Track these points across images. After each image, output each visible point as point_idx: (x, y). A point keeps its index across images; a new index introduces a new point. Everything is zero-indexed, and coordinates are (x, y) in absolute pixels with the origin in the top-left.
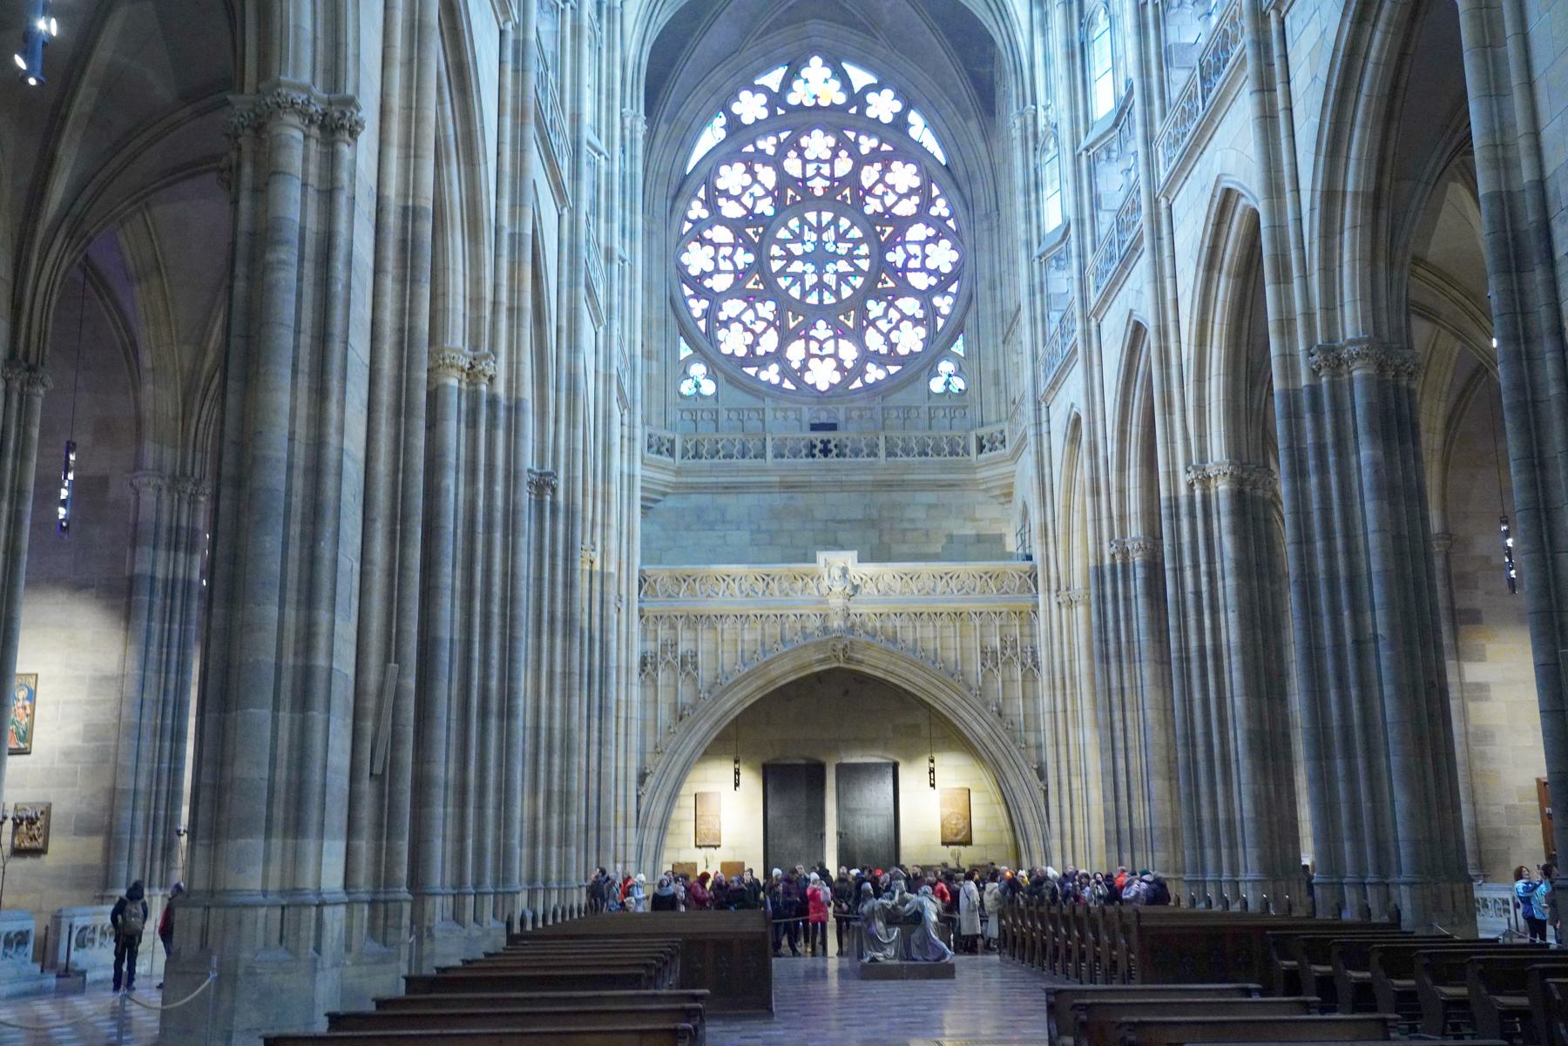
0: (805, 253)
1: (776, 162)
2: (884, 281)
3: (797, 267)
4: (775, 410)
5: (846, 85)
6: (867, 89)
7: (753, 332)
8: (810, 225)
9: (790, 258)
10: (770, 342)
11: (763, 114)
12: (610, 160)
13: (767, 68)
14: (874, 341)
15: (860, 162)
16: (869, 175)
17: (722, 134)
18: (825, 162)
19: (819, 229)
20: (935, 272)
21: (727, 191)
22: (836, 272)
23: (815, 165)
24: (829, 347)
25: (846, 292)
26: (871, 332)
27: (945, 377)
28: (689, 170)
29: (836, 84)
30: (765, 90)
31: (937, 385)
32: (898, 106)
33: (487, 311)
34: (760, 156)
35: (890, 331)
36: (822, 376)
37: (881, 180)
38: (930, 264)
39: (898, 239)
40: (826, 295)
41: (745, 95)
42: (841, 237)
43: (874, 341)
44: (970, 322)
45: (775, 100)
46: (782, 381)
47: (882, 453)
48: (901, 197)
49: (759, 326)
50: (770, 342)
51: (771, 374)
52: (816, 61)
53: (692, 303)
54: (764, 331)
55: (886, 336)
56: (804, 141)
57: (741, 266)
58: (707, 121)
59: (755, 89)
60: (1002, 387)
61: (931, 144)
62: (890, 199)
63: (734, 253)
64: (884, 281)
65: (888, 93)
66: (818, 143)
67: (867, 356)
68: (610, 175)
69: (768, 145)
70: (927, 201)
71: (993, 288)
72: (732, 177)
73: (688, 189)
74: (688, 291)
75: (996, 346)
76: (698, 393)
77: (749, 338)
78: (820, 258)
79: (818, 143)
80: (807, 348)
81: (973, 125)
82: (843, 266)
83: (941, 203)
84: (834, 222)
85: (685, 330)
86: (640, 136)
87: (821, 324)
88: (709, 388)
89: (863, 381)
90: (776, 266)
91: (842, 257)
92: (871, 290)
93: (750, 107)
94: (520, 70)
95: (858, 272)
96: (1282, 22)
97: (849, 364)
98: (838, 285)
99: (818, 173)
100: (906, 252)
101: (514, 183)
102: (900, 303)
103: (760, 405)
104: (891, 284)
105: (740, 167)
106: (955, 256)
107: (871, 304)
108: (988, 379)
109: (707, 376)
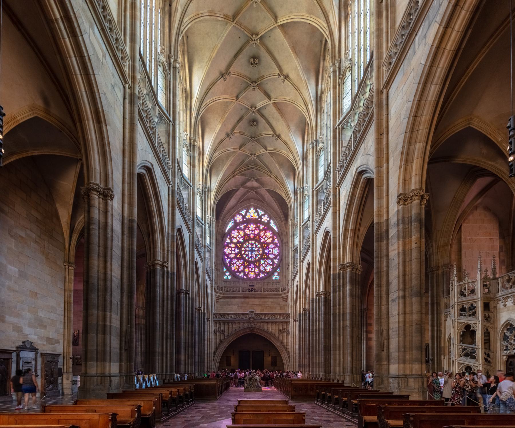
1: (243, 230)
5: (258, 214)
6: (263, 215)
11: (241, 220)
12: (205, 226)
15: (260, 231)
17: (233, 224)
29: (256, 214)
32: (268, 219)
33: (166, 252)
34: (240, 229)
41: (238, 216)
45: (244, 217)
56: (249, 226)
58: (230, 221)
65: (266, 216)
66: (252, 226)
68: (205, 229)
69: (242, 227)
72: (235, 233)
73: (226, 236)
79: (252, 226)
81: (283, 223)
86: (214, 223)
93: (239, 218)
94: (173, 197)
96: (339, 190)
101: (172, 223)
105: (236, 231)
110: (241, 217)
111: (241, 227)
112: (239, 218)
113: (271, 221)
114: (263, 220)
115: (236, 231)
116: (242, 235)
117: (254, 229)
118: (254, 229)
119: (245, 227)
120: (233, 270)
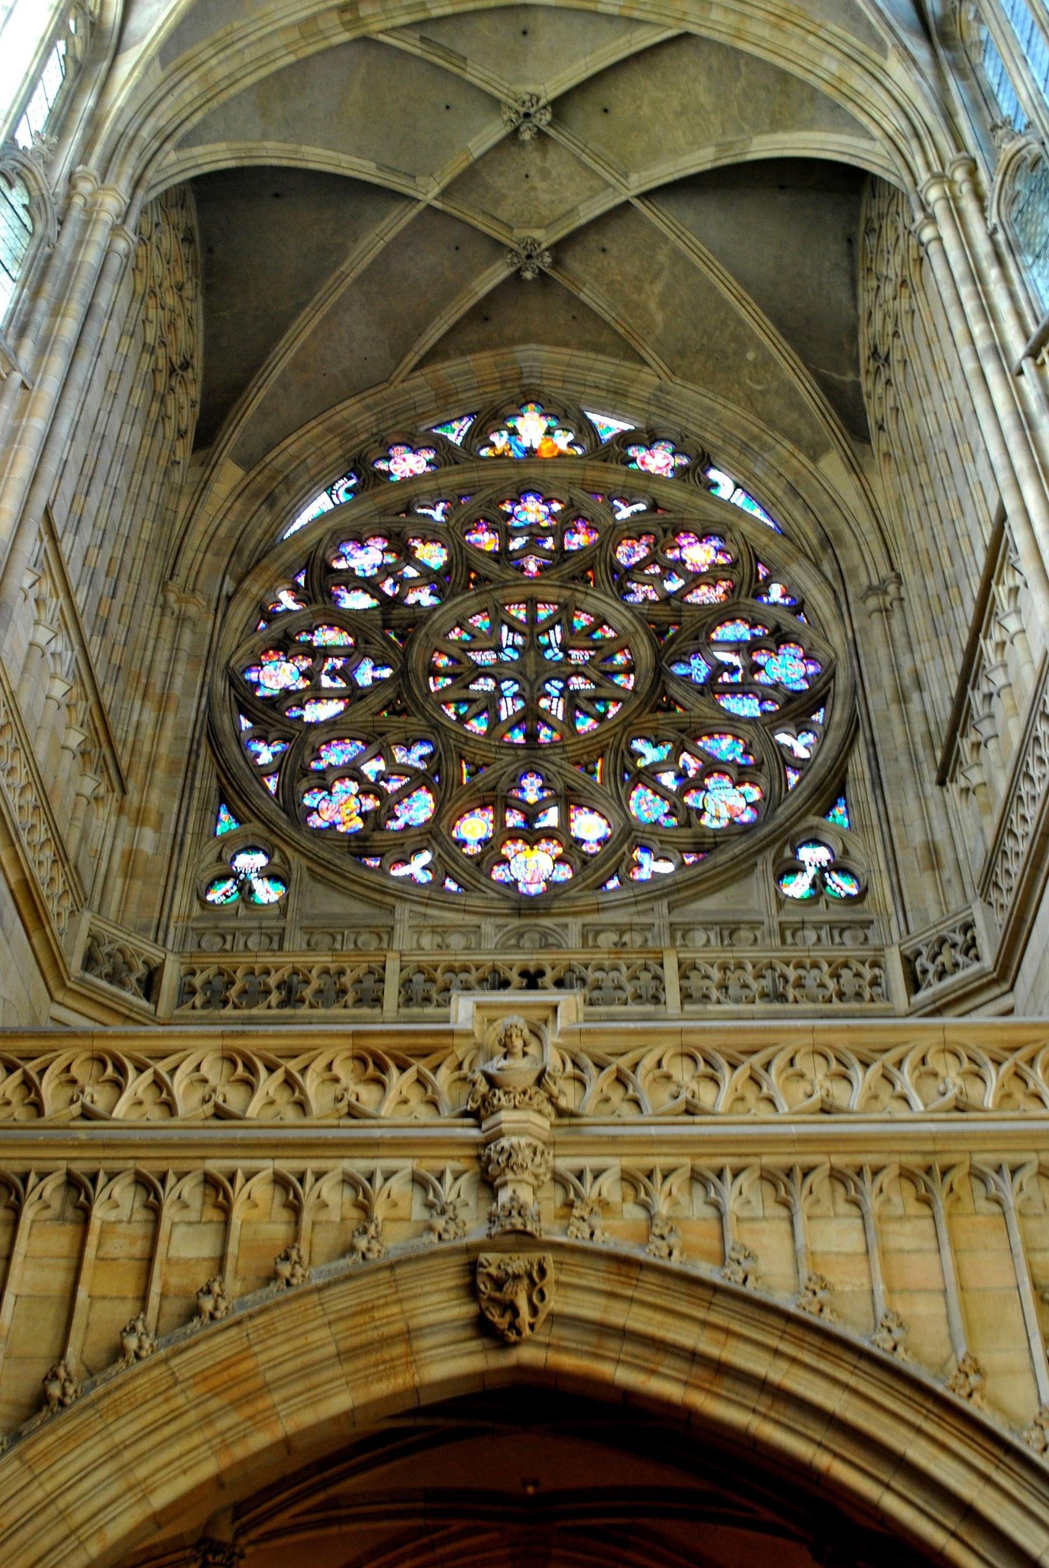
0: (500, 662)
4: (418, 930)
6: (624, 440)
7: (380, 794)
14: (646, 806)
24: (551, 818)
27: (811, 871)
31: (798, 887)
36: (532, 867)
44: (858, 763)
47: (672, 995)
50: (419, 808)
54: (405, 793)
60: (948, 873)
62: (673, 585)
67: (630, 836)
71: (902, 698)
75: (921, 797)
77: (370, 803)
79: (532, 511)
80: (499, 822)
85: (233, 789)
93: (407, 464)
98: (570, 719)
102: (705, 743)
103: (383, 920)
108: (909, 859)
112: (407, 464)
120: (315, 821)
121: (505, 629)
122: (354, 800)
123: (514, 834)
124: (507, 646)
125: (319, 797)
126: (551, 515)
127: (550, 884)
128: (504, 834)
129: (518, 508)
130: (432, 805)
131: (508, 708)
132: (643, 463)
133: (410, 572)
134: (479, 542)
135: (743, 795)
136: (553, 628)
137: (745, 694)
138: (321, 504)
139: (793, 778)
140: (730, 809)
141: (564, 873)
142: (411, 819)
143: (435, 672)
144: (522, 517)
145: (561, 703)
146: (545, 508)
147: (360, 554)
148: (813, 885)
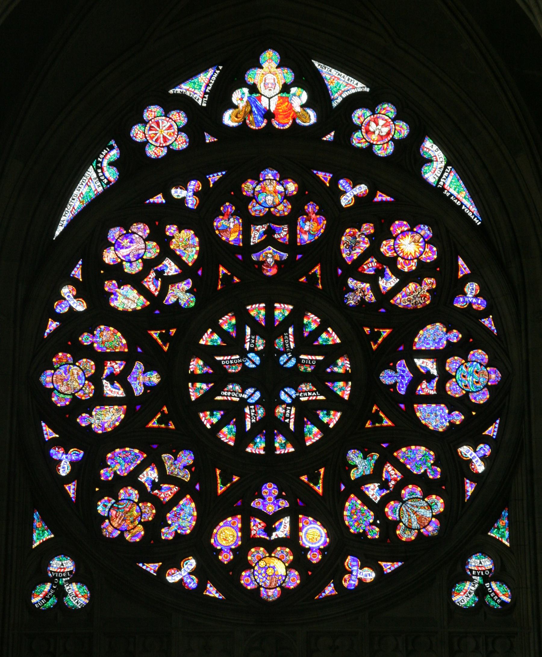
1: (200, 221)
2: (379, 419)
3: (232, 393)
6: (354, 102)
7: (155, 501)
8: (253, 322)
9: (219, 378)
10: (184, 518)
11: (181, 143)
13: (190, 74)
14: (357, 517)
15: (339, 220)
16: (354, 244)
17: (111, 174)
18: (281, 220)
19: (270, 330)
20: (462, 403)
21: (119, 266)
22: (296, 402)
23: (262, 228)
24: (283, 529)
25: (313, 434)
26: (354, 503)
27: (478, 579)
28: (57, 233)
29: (299, 97)
30: (185, 103)
31: (464, 596)
32: (403, 130)
34: (177, 213)
35: (385, 501)
37: (373, 251)
38: (453, 389)
39: (402, 347)
40: (279, 440)
41: (153, 112)
42: (306, 344)
43: (357, 517)
46: (202, 586)
48: (405, 279)
49: (167, 493)
50: (184, 518)
51: (184, 573)
52: (270, 58)
53: (57, 453)
54: (175, 500)
55: (378, 509)
56: (248, 187)
57: (138, 389)
59: (170, 104)
61: (455, 188)
62: (388, 283)
63: (127, 370)
64: (379, 419)
65: (388, 110)
67: (343, 543)
70: (449, 287)
74: (49, 433)
76: (61, 606)
77: (149, 512)
78: (270, 378)
79: (271, 192)
80: (245, 529)
82: (308, 393)
83: (472, 288)
84: (296, 319)
87: (270, 490)
88: (77, 595)
89: (338, 586)
90: (197, 390)
91: (306, 378)
92: (352, 433)
93: (161, 132)
95: (333, 402)
97: (315, 558)
98: (300, 424)
99: (269, 239)
100: (413, 368)
104: (387, 422)
105: (141, 230)
106: (495, 376)
107: (355, 457)
109: (75, 577)
110: (180, 118)
111: (177, 193)
113: (430, 147)
114: (358, 140)
115: (141, 230)
116: (191, 256)
117: (284, 209)
118: (284, 209)
119: (211, 203)
121: (248, 330)
122: (135, 507)
123: (258, 543)
124: (252, 350)
125: (109, 505)
126: (286, 197)
127: (285, 591)
128: (248, 541)
129: (258, 188)
130: (195, 514)
131: (252, 416)
132: (368, 132)
133: (171, 268)
134: (226, 229)
135: (430, 507)
136: (287, 331)
137: (438, 403)
138: (88, 188)
139: (470, 488)
140: (420, 518)
141: (294, 580)
142: (180, 527)
143: (195, 378)
144: (261, 198)
145: (293, 410)
146: (280, 188)
147: (125, 242)
148: (477, 593)
